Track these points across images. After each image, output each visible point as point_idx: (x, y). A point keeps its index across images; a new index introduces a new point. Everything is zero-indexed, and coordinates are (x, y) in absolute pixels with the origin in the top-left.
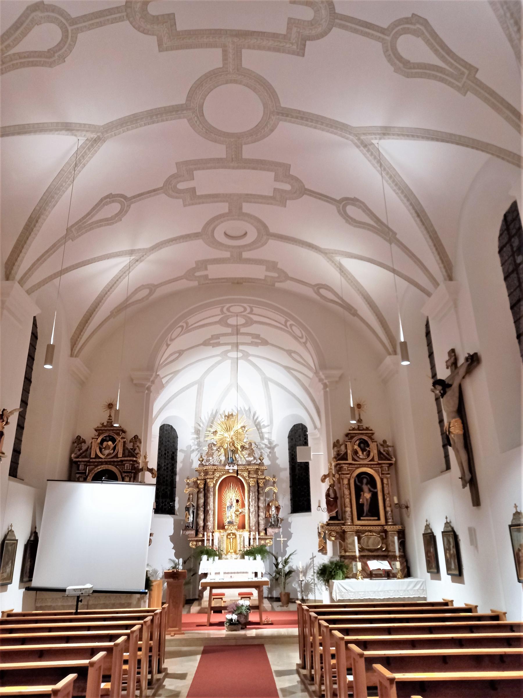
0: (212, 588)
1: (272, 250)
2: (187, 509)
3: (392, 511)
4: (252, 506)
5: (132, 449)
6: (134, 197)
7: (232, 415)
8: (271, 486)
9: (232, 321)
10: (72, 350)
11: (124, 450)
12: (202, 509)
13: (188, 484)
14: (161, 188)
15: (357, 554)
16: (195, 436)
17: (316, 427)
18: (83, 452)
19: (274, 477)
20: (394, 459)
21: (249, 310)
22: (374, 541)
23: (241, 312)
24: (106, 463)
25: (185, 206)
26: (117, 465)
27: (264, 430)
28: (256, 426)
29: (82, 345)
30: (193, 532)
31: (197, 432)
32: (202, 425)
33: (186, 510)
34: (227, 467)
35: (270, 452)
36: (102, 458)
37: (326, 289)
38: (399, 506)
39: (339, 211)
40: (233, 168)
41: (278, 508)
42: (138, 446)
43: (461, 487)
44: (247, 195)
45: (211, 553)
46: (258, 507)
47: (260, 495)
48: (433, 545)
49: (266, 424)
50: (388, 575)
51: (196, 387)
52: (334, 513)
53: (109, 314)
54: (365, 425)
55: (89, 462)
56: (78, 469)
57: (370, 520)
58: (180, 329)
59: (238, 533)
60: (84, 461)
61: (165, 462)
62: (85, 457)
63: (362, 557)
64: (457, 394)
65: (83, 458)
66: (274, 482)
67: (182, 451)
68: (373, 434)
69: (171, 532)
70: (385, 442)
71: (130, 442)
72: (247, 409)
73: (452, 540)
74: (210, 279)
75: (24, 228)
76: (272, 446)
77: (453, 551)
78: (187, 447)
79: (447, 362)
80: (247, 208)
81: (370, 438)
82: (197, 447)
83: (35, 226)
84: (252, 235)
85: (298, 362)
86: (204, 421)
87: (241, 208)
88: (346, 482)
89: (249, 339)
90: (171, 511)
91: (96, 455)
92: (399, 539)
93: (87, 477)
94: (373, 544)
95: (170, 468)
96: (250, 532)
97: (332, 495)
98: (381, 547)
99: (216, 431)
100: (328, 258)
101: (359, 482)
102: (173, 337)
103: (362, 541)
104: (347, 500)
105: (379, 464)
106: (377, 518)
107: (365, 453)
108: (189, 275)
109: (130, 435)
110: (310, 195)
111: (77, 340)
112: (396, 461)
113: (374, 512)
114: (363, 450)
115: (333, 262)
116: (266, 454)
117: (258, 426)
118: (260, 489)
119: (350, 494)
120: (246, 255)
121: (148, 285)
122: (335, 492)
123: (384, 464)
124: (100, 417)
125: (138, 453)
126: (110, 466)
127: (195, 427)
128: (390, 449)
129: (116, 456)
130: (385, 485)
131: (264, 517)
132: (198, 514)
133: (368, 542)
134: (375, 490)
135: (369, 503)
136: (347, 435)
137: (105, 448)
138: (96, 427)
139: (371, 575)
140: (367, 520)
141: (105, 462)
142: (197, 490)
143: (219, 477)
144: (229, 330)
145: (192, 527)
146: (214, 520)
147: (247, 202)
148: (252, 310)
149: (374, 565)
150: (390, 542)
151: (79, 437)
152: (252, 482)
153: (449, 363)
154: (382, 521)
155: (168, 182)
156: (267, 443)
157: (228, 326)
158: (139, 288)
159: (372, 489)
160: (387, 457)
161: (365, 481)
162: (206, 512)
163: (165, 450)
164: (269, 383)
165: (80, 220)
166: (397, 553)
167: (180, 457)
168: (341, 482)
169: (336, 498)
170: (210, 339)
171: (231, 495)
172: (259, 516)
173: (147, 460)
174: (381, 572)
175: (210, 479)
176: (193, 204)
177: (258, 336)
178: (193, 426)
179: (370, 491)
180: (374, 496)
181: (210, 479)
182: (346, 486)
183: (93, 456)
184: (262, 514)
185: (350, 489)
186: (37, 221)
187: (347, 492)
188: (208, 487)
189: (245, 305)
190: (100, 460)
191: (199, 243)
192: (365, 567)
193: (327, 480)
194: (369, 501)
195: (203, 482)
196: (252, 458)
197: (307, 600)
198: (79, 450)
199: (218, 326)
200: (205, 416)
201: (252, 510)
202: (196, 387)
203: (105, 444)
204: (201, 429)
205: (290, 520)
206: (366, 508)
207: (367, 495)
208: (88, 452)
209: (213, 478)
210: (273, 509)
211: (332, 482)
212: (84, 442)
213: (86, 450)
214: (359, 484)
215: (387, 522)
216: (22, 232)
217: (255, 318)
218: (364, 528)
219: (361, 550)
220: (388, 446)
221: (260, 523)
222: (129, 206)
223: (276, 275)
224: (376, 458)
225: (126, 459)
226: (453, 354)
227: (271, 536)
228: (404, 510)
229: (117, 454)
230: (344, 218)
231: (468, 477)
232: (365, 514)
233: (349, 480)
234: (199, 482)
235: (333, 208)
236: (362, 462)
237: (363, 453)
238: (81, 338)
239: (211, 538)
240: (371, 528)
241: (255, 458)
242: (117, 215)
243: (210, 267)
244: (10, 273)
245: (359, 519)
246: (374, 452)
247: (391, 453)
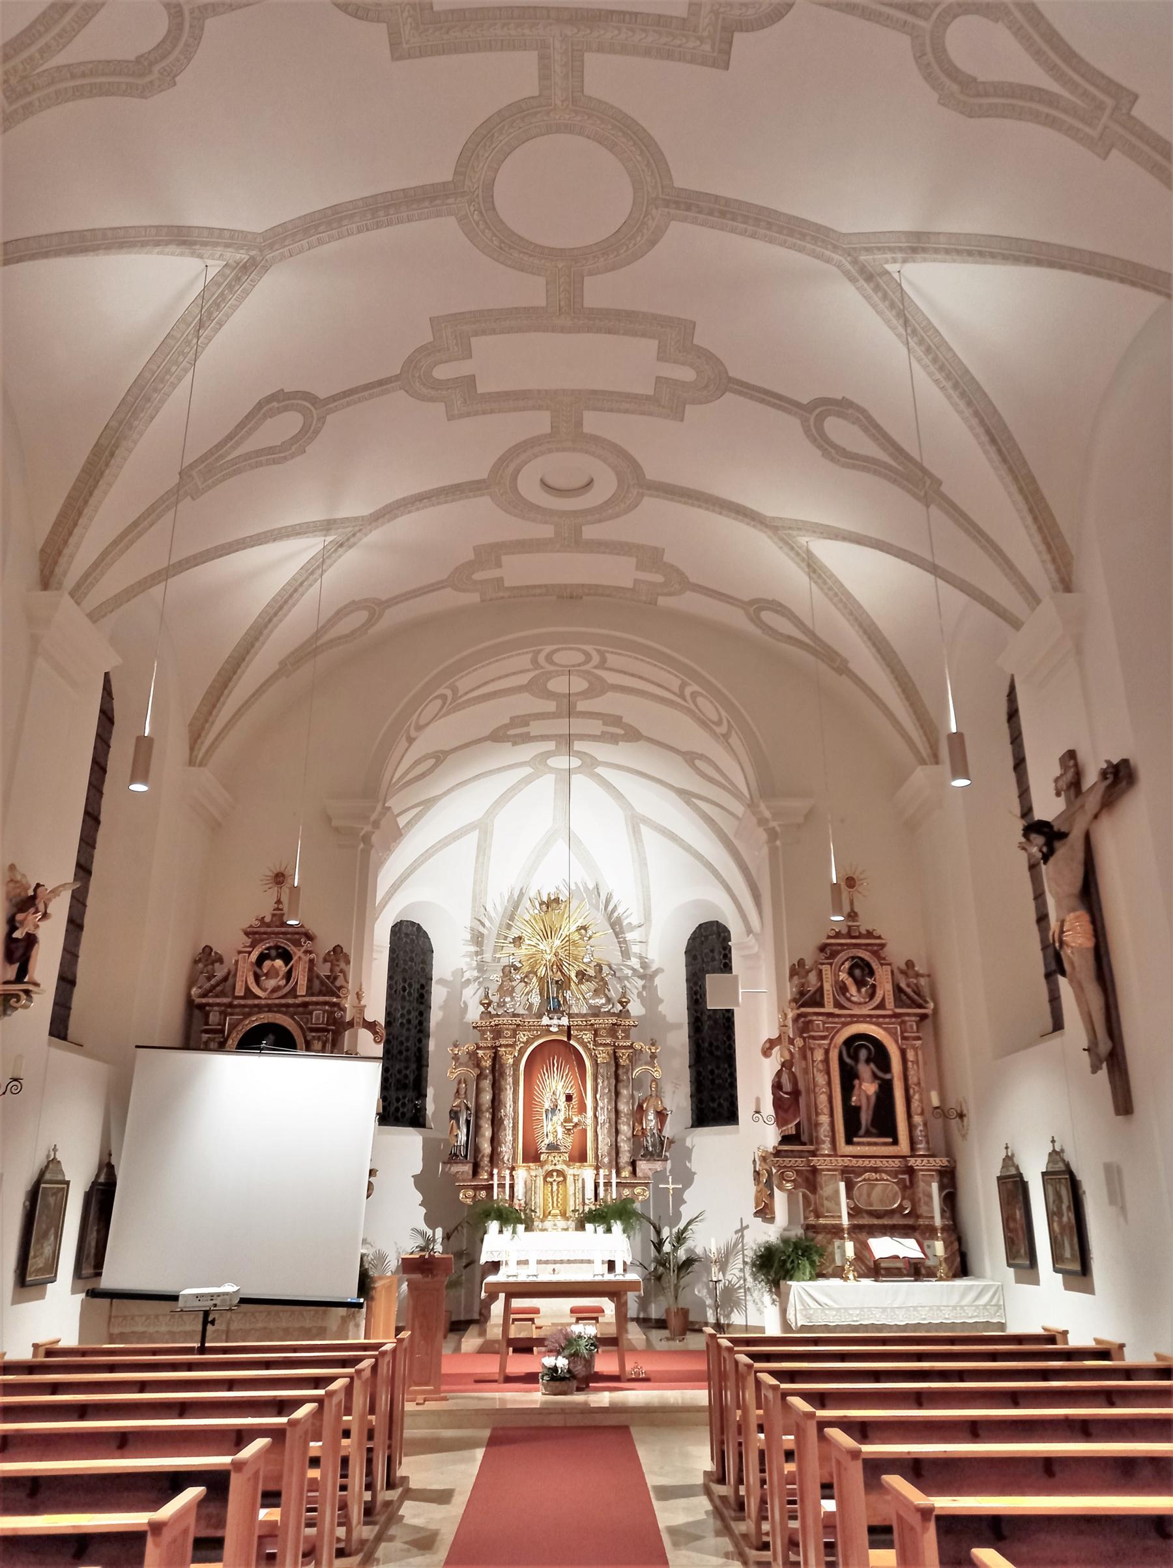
0: (510, 1296)
1: (653, 521)
2: (454, 1115)
3: (925, 1125)
4: (602, 1108)
5: (328, 977)
6: (334, 398)
7: (557, 900)
8: (646, 1064)
9: (558, 685)
10: (192, 749)
11: (310, 980)
12: (488, 1115)
13: (456, 1058)
14: (397, 378)
15: (845, 1221)
16: (473, 949)
17: (749, 931)
18: (218, 984)
19: (653, 1045)
20: (931, 1005)
21: (596, 659)
22: (883, 1193)
23: (579, 665)
24: (270, 1008)
25: (450, 418)
26: (295, 1014)
27: (629, 936)
28: (613, 926)
29: (216, 739)
30: (467, 1168)
31: (478, 939)
32: (487, 923)
33: (451, 1118)
34: (545, 1021)
35: (644, 987)
36: (259, 998)
37: (777, 612)
38: (942, 1112)
39: (807, 431)
40: (563, 330)
41: (661, 1115)
42: (341, 971)
43: (1089, 1069)
44: (594, 392)
45: (508, 1217)
46: (617, 1112)
47: (620, 1085)
48: (1021, 1205)
49: (635, 922)
50: (916, 1270)
51: (475, 835)
52: (791, 1129)
53: (277, 667)
54: (864, 925)
55: (230, 1005)
56: (207, 1024)
57: (875, 1144)
58: (439, 702)
59: (570, 1172)
60: (218, 1005)
61: (403, 1008)
62: (223, 994)
63: (855, 1229)
64: (1080, 855)
65: (217, 996)
66: (653, 1056)
67: (441, 981)
68: (883, 946)
69: (418, 1168)
70: (910, 964)
71: (325, 960)
72: (591, 886)
73: (1065, 1193)
74: (508, 588)
75: (83, 471)
76: (649, 972)
77: (1068, 1217)
78: (454, 973)
79: (1056, 780)
80: (593, 422)
81: (875, 954)
82: (476, 973)
83: (107, 464)
84: (606, 486)
85: (711, 780)
86: (493, 914)
87: (579, 424)
88: (819, 1055)
89: (596, 727)
90: (417, 1120)
91: (248, 989)
92: (941, 1188)
93: (226, 1040)
94: (882, 1201)
95: (415, 1022)
96: (597, 1168)
97: (788, 1087)
98: (900, 1205)
99: (520, 938)
100: (782, 539)
101: (849, 1056)
102: (422, 722)
103: (855, 1192)
104: (823, 1099)
105: (895, 1015)
106: (890, 1140)
107: (863, 990)
108: (460, 578)
109: (325, 945)
110: (740, 393)
111: (203, 728)
112: (936, 1011)
113: (884, 1125)
114: (860, 984)
115: (792, 548)
116: (635, 992)
117: (617, 926)
118: (620, 1071)
119: (829, 1083)
120: (590, 532)
121: (366, 600)
122: (794, 1080)
123: (908, 1015)
124: (256, 905)
125: (341, 987)
126: (278, 1015)
127: (472, 929)
128: (923, 981)
129: (293, 993)
130: (910, 1064)
131: (629, 1134)
132: (478, 1127)
133: (869, 1195)
134: (888, 1077)
136: (823, 948)
137: (266, 975)
138: (245, 925)
139: (877, 1270)
140: (869, 1144)
141: (268, 1005)
142: (476, 1072)
143: (528, 1043)
144: (551, 706)
145: (466, 1156)
146: (515, 1140)
147: (595, 409)
148: (604, 660)
149: (883, 1247)
150: (921, 1195)
151: (208, 950)
152: (603, 1056)
153: (1063, 784)
154: (904, 1146)
155: (411, 363)
156: (637, 967)
157: (551, 695)
158: (345, 607)
159: (880, 1074)
160: (916, 1000)
162: (497, 1123)
163: (405, 981)
164: (644, 829)
165: (211, 452)
166: (938, 1222)
167: (438, 995)
169: (796, 1093)
170: (506, 727)
171: (555, 1085)
172: (617, 1132)
173: (363, 1003)
174: (900, 1265)
175: (507, 1046)
176: (468, 415)
177: (617, 721)
178: (469, 925)
179: (875, 1076)
180: (886, 1089)
181: (507, 1046)
182: (821, 1066)
183: (239, 992)
184: (625, 1129)
185: (828, 1073)
186: (112, 455)
187: (821, 1079)
188: (502, 1066)
189: (588, 648)
190: (256, 1002)
191: (483, 503)
192: (862, 1251)
193: (776, 1051)
194: (873, 1100)
195: (490, 1053)
196: (603, 1001)
197: (729, 1325)
198: (209, 979)
199: (525, 696)
200: (496, 903)
201: (601, 1119)
202: (475, 835)
203: (267, 964)
204: (485, 931)
205: (688, 1143)
206: (865, 1118)
207: (868, 1088)
208: (231, 979)
209: (513, 1046)
210: (651, 1116)
211: (788, 1057)
212: (220, 960)
213: (225, 979)
214: (848, 1060)
216: (78, 480)
217: (612, 678)
219: (854, 1212)
220: (917, 975)
221: (622, 1149)
222: (322, 419)
223: (659, 578)
224: (890, 1002)
225: (314, 999)
226: (1072, 763)
227: (645, 1178)
228: (954, 1123)
229: (294, 989)
230: (820, 447)
231: (1105, 1046)
233: (827, 1052)
234: (481, 1053)
235: (793, 423)
237: (859, 991)
238: (213, 723)
239: (508, 1182)
240: (878, 1163)
241: (609, 1000)
242: (295, 439)
243: (505, 559)
244: (52, 572)
245: (849, 1142)
246: (885, 989)
247: (926, 991)
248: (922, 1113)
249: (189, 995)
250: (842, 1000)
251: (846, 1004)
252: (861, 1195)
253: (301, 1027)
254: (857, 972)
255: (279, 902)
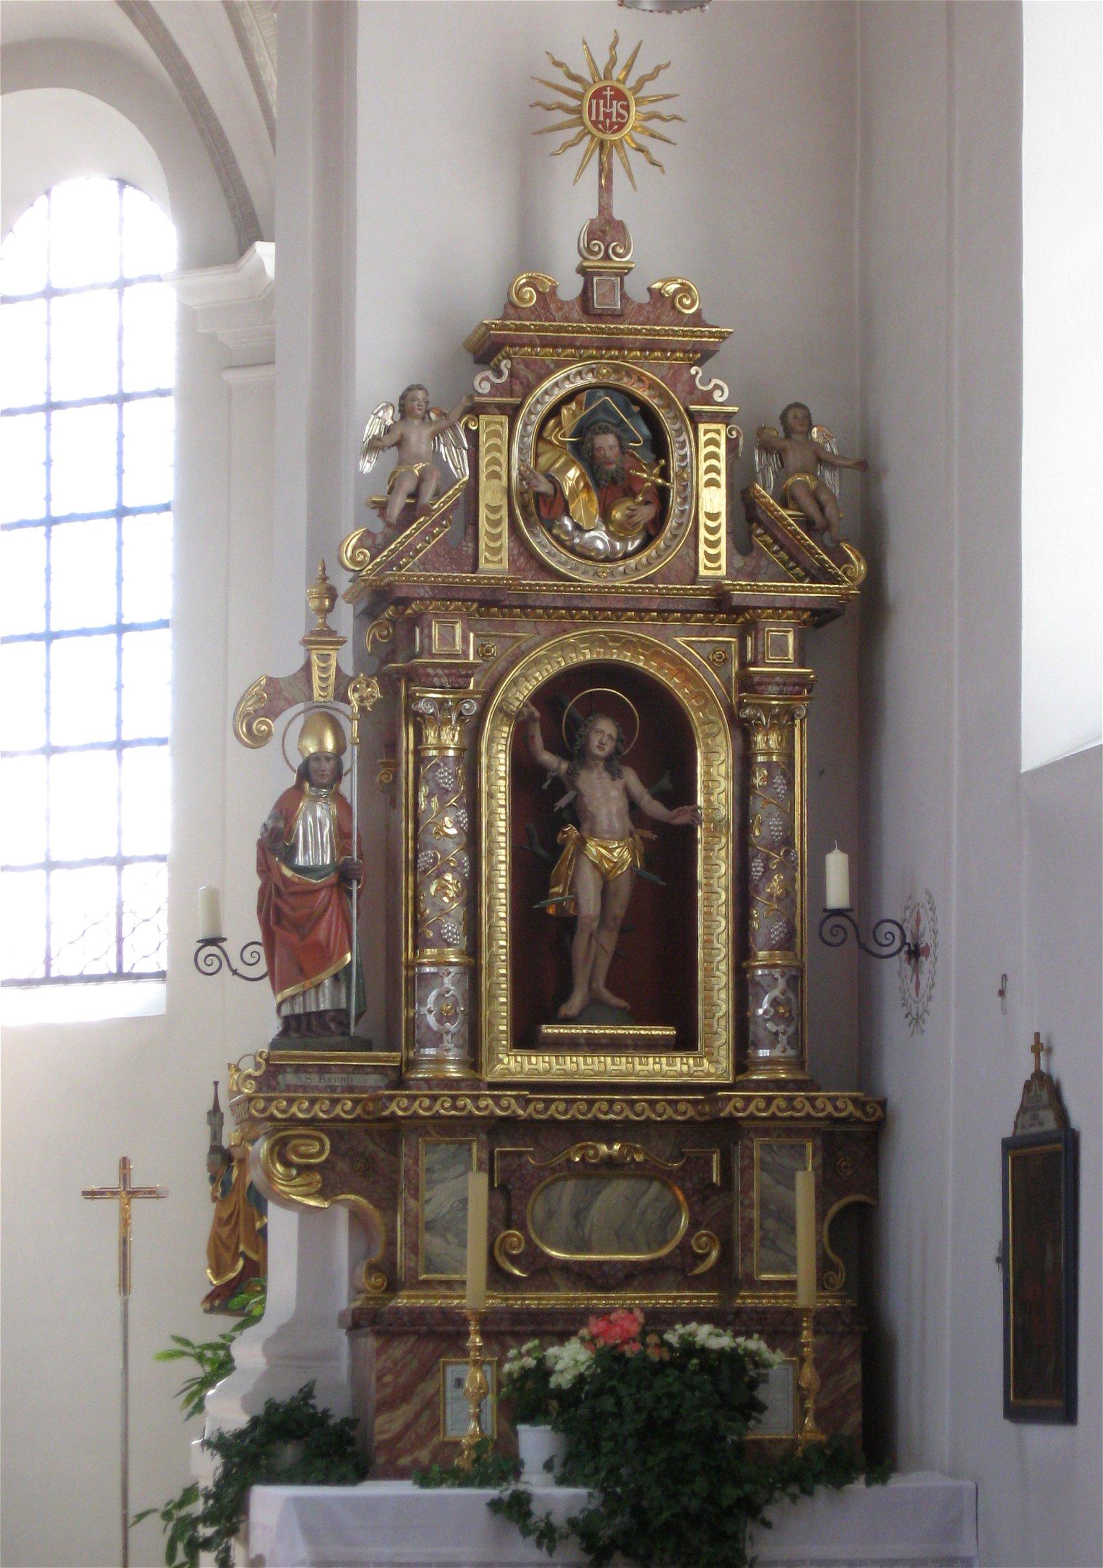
3: (795, 981)
15: (474, 1295)
57: (615, 1046)
92: (826, 1190)
98: (684, 1246)
104: (445, 892)
106: (670, 1032)
114: (609, 486)
133: (579, 1215)
134: (679, 817)
135: (619, 909)
136: (486, 350)
140: (595, 1045)
159: (655, 808)
161: (603, 734)
166: (806, 1296)
168: (408, 739)
169: (344, 875)
180: (669, 854)
194: (623, 892)
206: (593, 956)
207: (609, 851)
214: (547, 758)
215: (742, 1063)
218: (558, 1110)
220: (821, 460)
224: (714, 559)
232: (575, 1003)
236: (586, 577)
245: (525, 1038)
247: (840, 515)
248: (787, 943)
250: (541, 543)
251: (558, 560)
252: (550, 1214)
254: (607, 443)
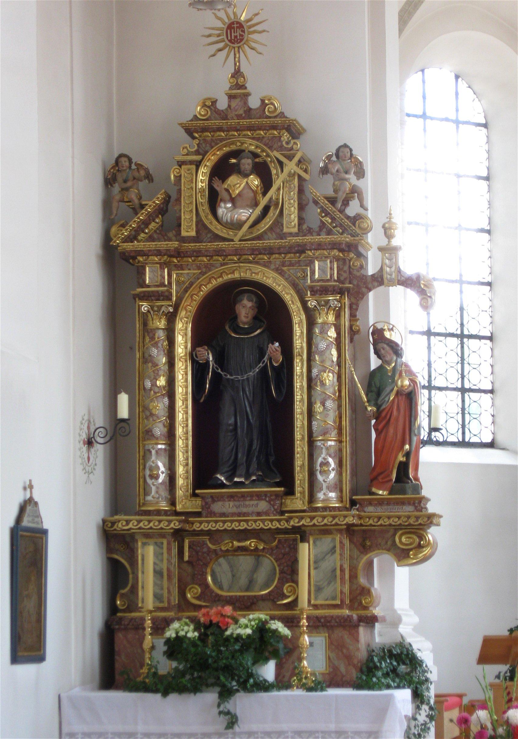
5: (332, 201)
18: (150, 218)
55: (178, 254)
56: (143, 284)
60: (159, 253)
62: (162, 233)
65: (151, 239)
173: (395, 242)
183: (188, 230)
212: (149, 177)
213: (162, 210)
249: (107, 239)
253: (295, 286)
255: (237, 73)
